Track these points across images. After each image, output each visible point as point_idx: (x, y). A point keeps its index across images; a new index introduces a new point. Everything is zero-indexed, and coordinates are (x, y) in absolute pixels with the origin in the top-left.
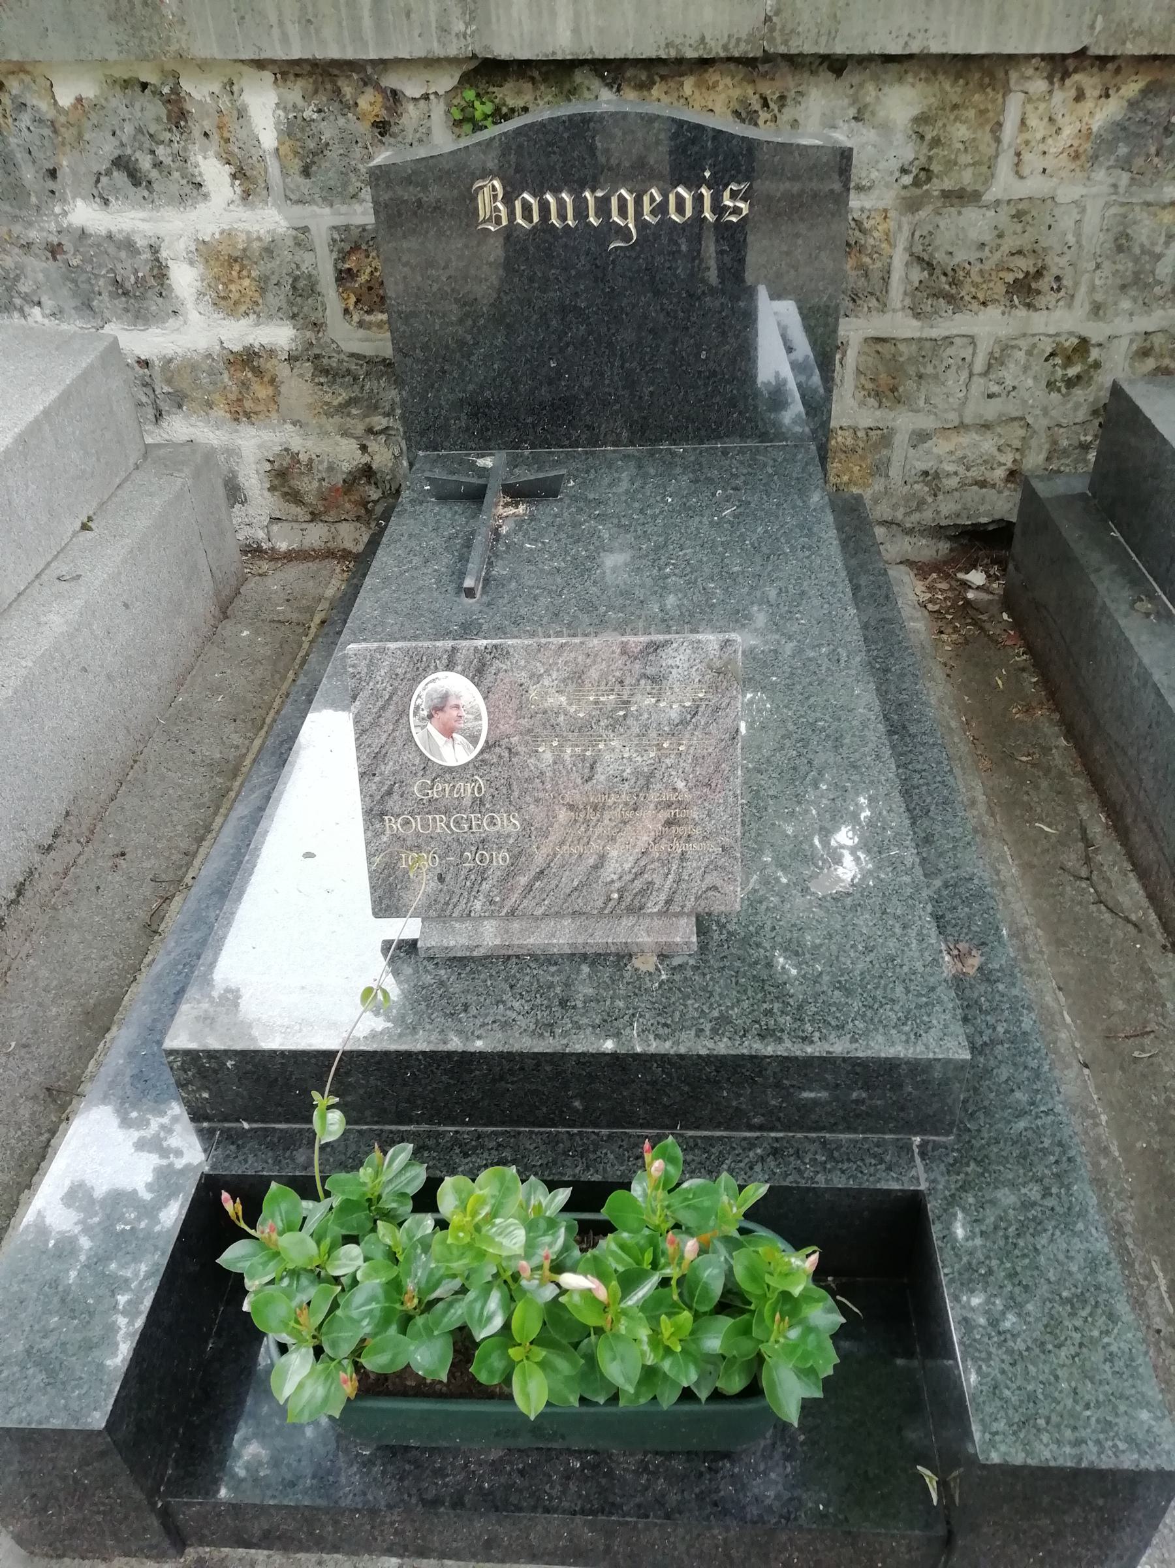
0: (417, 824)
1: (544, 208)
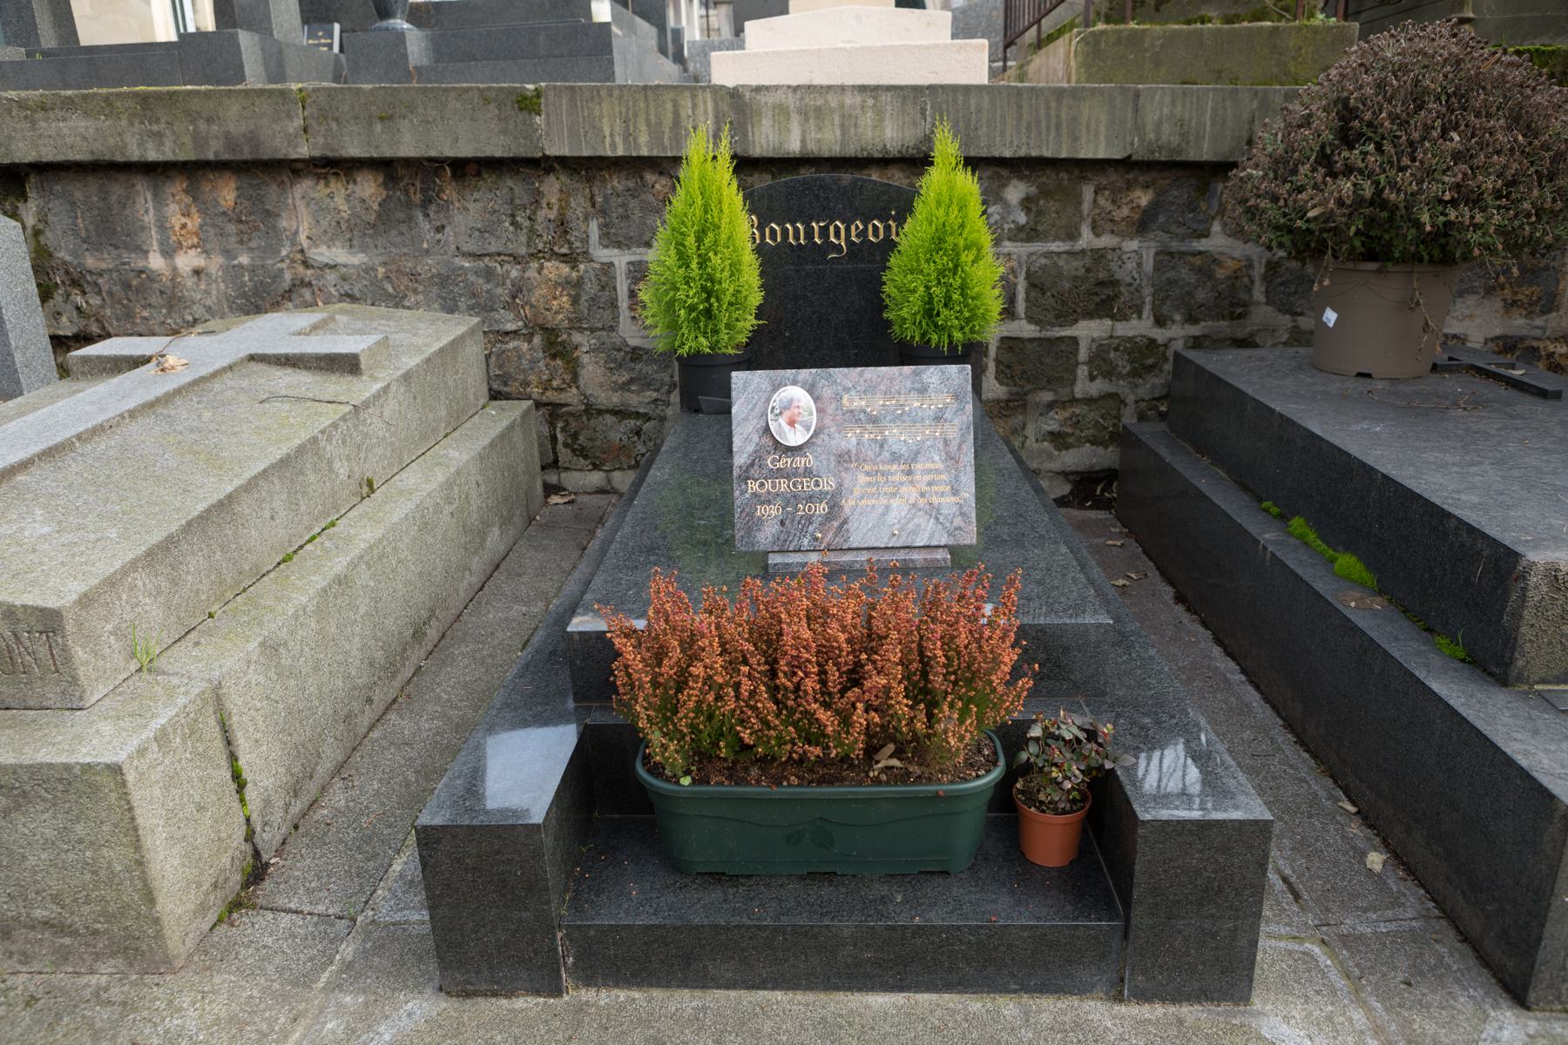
0: (768, 485)
1: (785, 232)
